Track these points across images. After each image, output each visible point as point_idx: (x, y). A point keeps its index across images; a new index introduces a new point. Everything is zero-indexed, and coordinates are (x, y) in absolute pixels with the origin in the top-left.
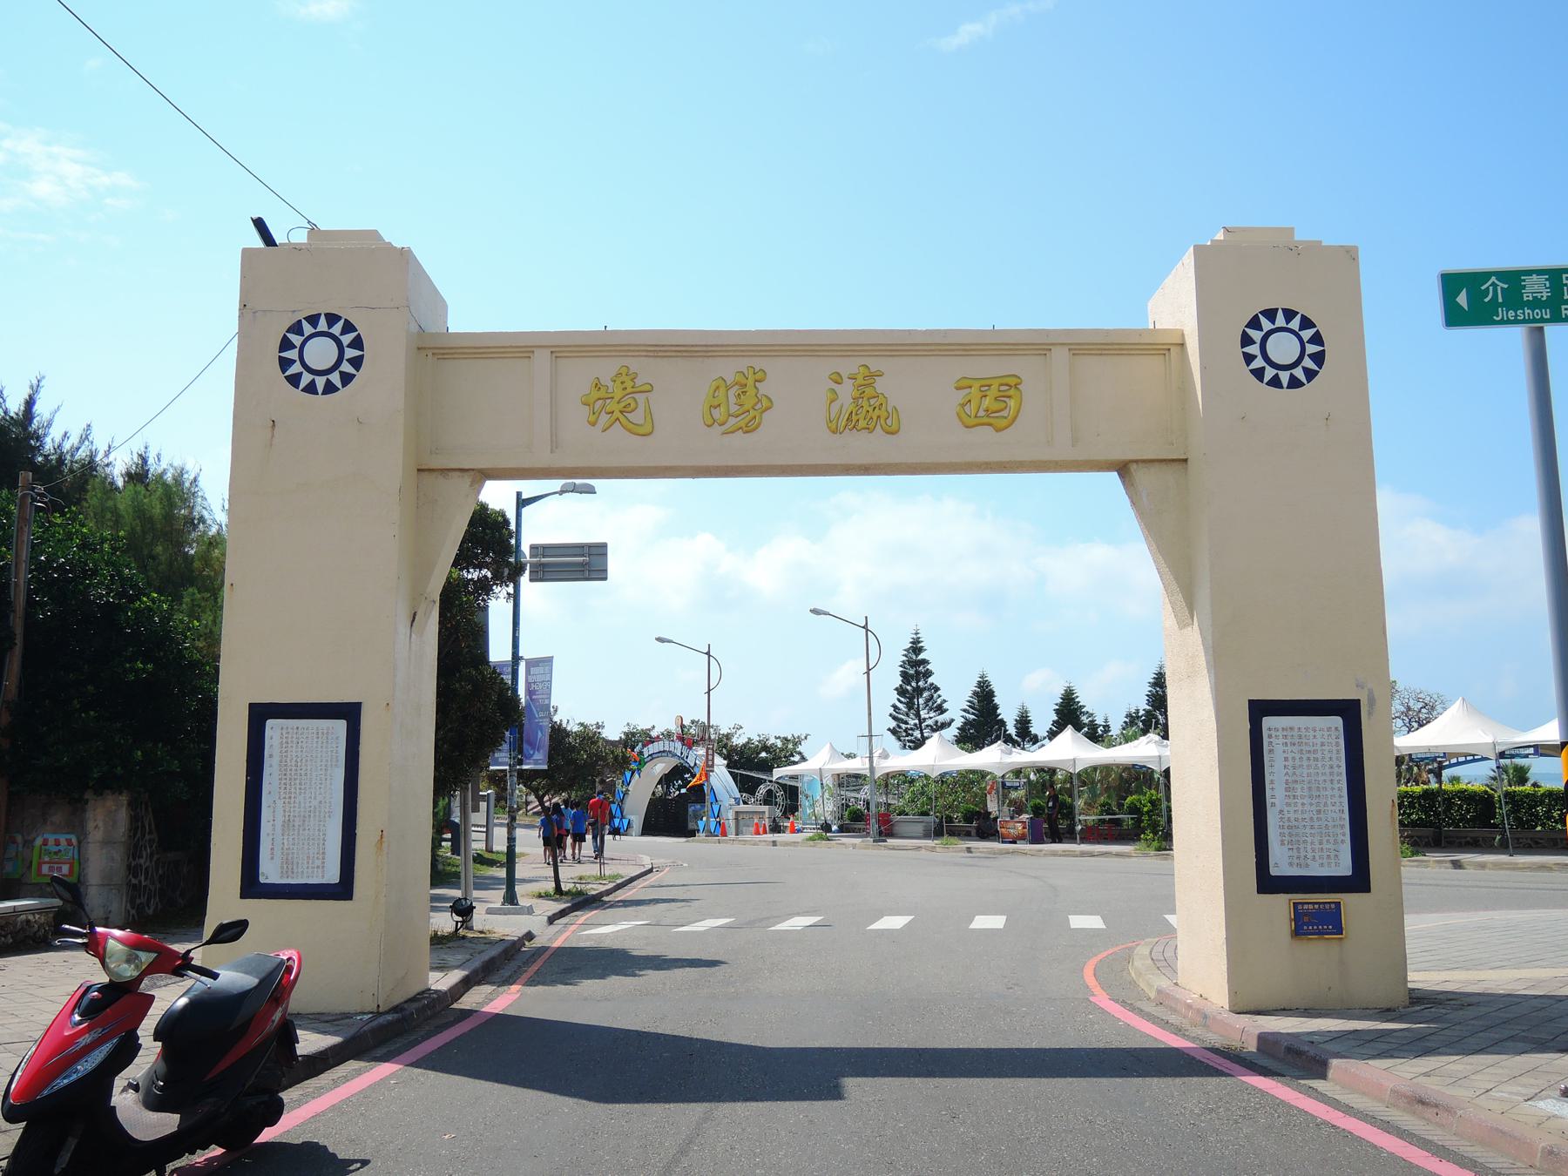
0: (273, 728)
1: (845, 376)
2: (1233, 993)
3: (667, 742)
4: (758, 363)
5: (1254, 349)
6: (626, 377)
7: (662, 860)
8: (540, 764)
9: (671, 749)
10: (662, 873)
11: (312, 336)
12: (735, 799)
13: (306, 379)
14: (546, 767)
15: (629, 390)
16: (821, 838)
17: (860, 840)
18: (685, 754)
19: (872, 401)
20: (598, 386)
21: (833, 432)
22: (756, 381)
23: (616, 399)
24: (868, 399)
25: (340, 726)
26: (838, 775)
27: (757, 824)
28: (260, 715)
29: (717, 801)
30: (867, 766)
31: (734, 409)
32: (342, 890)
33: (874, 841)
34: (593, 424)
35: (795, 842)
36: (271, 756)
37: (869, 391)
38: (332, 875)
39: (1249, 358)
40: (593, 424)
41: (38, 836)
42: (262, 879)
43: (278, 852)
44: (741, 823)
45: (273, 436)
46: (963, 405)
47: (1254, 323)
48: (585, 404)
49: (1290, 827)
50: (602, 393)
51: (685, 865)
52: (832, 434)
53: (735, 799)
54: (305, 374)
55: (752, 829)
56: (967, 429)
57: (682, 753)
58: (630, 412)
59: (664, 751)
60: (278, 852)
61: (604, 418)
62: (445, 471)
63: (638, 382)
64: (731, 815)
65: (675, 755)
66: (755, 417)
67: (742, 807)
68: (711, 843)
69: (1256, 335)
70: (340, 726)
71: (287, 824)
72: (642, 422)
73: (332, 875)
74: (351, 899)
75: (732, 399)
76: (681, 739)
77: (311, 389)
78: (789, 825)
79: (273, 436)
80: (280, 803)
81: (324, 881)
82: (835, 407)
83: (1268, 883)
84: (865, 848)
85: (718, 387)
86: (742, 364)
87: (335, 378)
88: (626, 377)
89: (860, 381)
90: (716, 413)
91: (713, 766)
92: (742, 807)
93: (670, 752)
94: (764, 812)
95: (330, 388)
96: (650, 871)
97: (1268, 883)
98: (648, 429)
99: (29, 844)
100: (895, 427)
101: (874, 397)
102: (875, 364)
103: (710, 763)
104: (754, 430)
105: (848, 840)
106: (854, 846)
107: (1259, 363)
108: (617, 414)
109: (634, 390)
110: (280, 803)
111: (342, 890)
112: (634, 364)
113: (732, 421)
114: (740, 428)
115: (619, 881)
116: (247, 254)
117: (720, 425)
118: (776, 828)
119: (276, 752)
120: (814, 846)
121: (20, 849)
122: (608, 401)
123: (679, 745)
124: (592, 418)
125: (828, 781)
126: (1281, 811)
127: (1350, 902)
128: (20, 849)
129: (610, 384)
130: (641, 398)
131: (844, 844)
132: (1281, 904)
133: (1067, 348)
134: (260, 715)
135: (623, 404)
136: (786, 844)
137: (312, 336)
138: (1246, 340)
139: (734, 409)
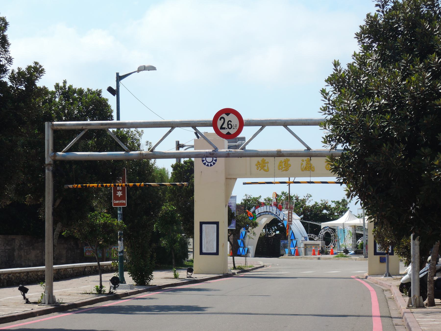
1: (304, 160)
2: (369, 272)
3: (268, 207)
7: (268, 264)
8: (233, 227)
9: (271, 211)
10: (268, 267)
12: (305, 237)
13: (207, 164)
14: (235, 228)
15: (264, 163)
16: (342, 256)
17: (358, 257)
18: (278, 213)
19: (310, 165)
20: (258, 162)
21: (302, 171)
22: (288, 161)
23: (262, 164)
25: (215, 226)
26: (355, 226)
27: (314, 250)
28: (201, 223)
29: (295, 238)
30: (362, 222)
31: (284, 166)
32: (217, 253)
33: (365, 257)
34: (258, 170)
35: (329, 258)
36: (204, 231)
37: (309, 163)
38: (215, 251)
40: (258, 170)
41: (113, 247)
42: (203, 252)
43: (205, 247)
44: (307, 249)
45: (201, 174)
46: (326, 166)
48: (256, 166)
51: (277, 265)
52: (301, 171)
53: (305, 237)
54: (207, 163)
55: (312, 252)
57: (276, 213)
59: (267, 212)
60: (205, 247)
61: (260, 168)
62: (230, 179)
63: (266, 162)
64: (302, 245)
65: (272, 214)
66: (288, 168)
67: (309, 242)
68: (291, 258)
70: (215, 226)
71: (207, 242)
72: (266, 169)
73: (215, 251)
75: (283, 165)
76: (276, 205)
77: (208, 165)
78: (330, 250)
79: (201, 174)
80: (205, 239)
81: (214, 252)
82: (303, 166)
84: (360, 260)
85: (281, 163)
87: (212, 163)
88: (263, 161)
89: (307, 161)
90: (280, 167)
91: (291, 221)
92: (309, 242)
93: (270, 212)
94: (319, 244)
95: (211, 165)
96: (263, 266)
99: (111, 249)
100: (314, 170)
103: (290, 220)
104: (288, 170)
105: (357, 257)
106: (356, 259)
108: (262, 167)
110: (205, 239)
111: (217, 253)
112: (265, 158)
113: (283, 169)
115: (253, 268)
116: (195, 140)
117: (281, 169)
118: (322, 252)
119: (204, 230)
120: (338, 260)
121: (108, 250)
123: (275, 208)
124: (258, 168)
125: (348, 229)
128: (108, 250)
129: (261, 162)
130: (266, 164)
131: (351, 259)
132: (378, 257)
134: (201, 223)
135: (263, 166)
136: (326, 259)
139: (284, 166)
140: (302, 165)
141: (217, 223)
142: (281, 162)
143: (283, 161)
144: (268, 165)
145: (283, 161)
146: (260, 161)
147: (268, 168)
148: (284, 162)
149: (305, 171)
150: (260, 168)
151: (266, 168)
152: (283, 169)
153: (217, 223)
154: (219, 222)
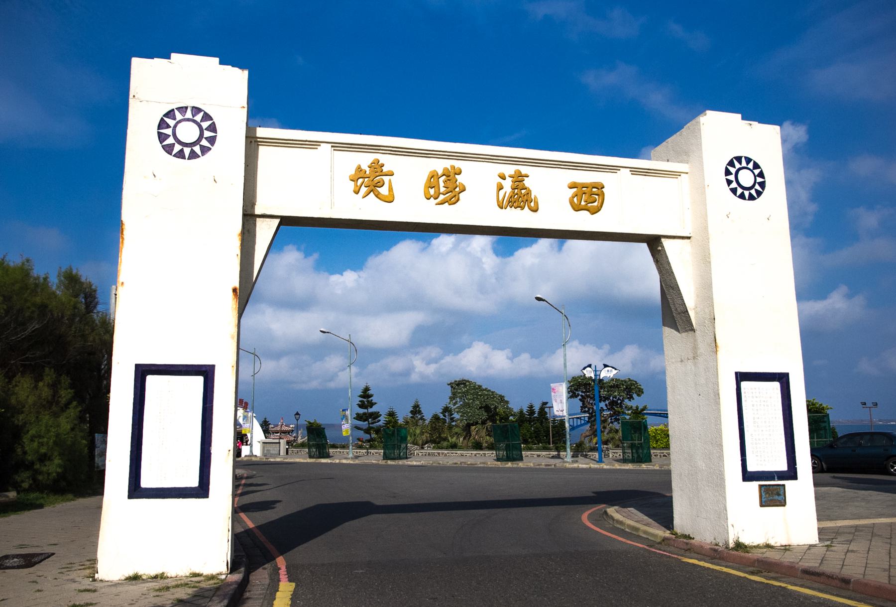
0: (152, 381)
4: (458, 164)
5: (732, 178)
6: (377, 167)
11: (188, 120)
20: (359, 169)
22: (456, 174)
23: (371, 178)
24: (521, 190)
28: (142, 372)
34: (357, 192)
39: (729, 182)
40: (357, 192)
47: (731, 163)
48: (351, 180)
49: (756, 444)
50: (362, 174)
56: (574, 211)
58: (380, 187)
61: (364, 190)
63: (385, 169)
69: (733, 170)
74: (208, 497)
82: (502, 193)
83: (748, 476)
86: (448, 164)
88: (377, 167)
90: (432, 191)
97: (748, 476)
98: (391, 199)
101: (524, 189)
102: (524, 170)
107: (734, 185)
109: (381, 174)
114: (447, 202)
122: (366, 180)
126: (752, 435)
127: (788, 484)
130: (386, 179)
132: (755, 485)
133: (629, 169)
134: (142, 372)
137: (188, 120)
138: (728, 173)
140: (500, 188)
141: (207, 373)
142: (433, 176)
143: (440, 172)
144: (390, 181)
145: (440, 172)
146: (365, 167)
147: (391, 189)
148: (444, 177)
149: (509, 207)
150: (364, 190)
151: (384, 191)
152: (442, 197)
153: (207, 373)
154: (214, 366)
